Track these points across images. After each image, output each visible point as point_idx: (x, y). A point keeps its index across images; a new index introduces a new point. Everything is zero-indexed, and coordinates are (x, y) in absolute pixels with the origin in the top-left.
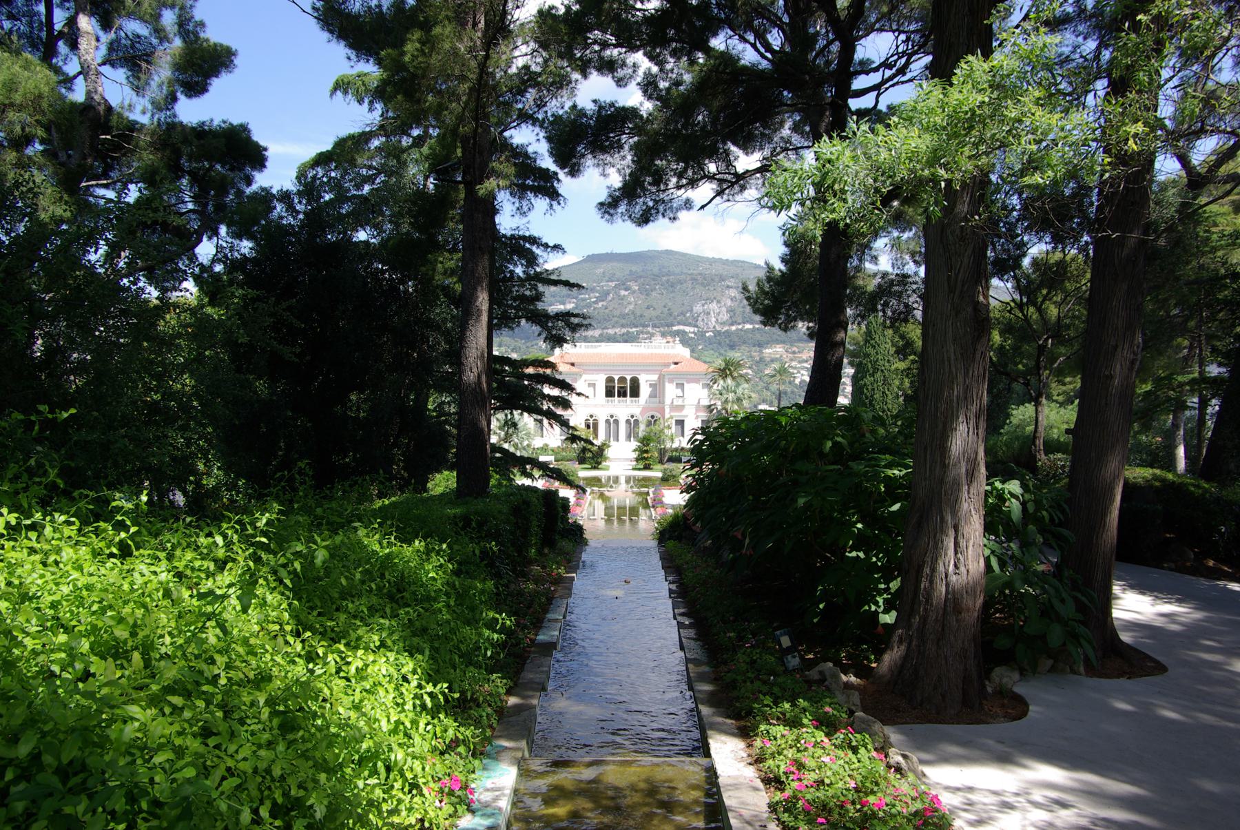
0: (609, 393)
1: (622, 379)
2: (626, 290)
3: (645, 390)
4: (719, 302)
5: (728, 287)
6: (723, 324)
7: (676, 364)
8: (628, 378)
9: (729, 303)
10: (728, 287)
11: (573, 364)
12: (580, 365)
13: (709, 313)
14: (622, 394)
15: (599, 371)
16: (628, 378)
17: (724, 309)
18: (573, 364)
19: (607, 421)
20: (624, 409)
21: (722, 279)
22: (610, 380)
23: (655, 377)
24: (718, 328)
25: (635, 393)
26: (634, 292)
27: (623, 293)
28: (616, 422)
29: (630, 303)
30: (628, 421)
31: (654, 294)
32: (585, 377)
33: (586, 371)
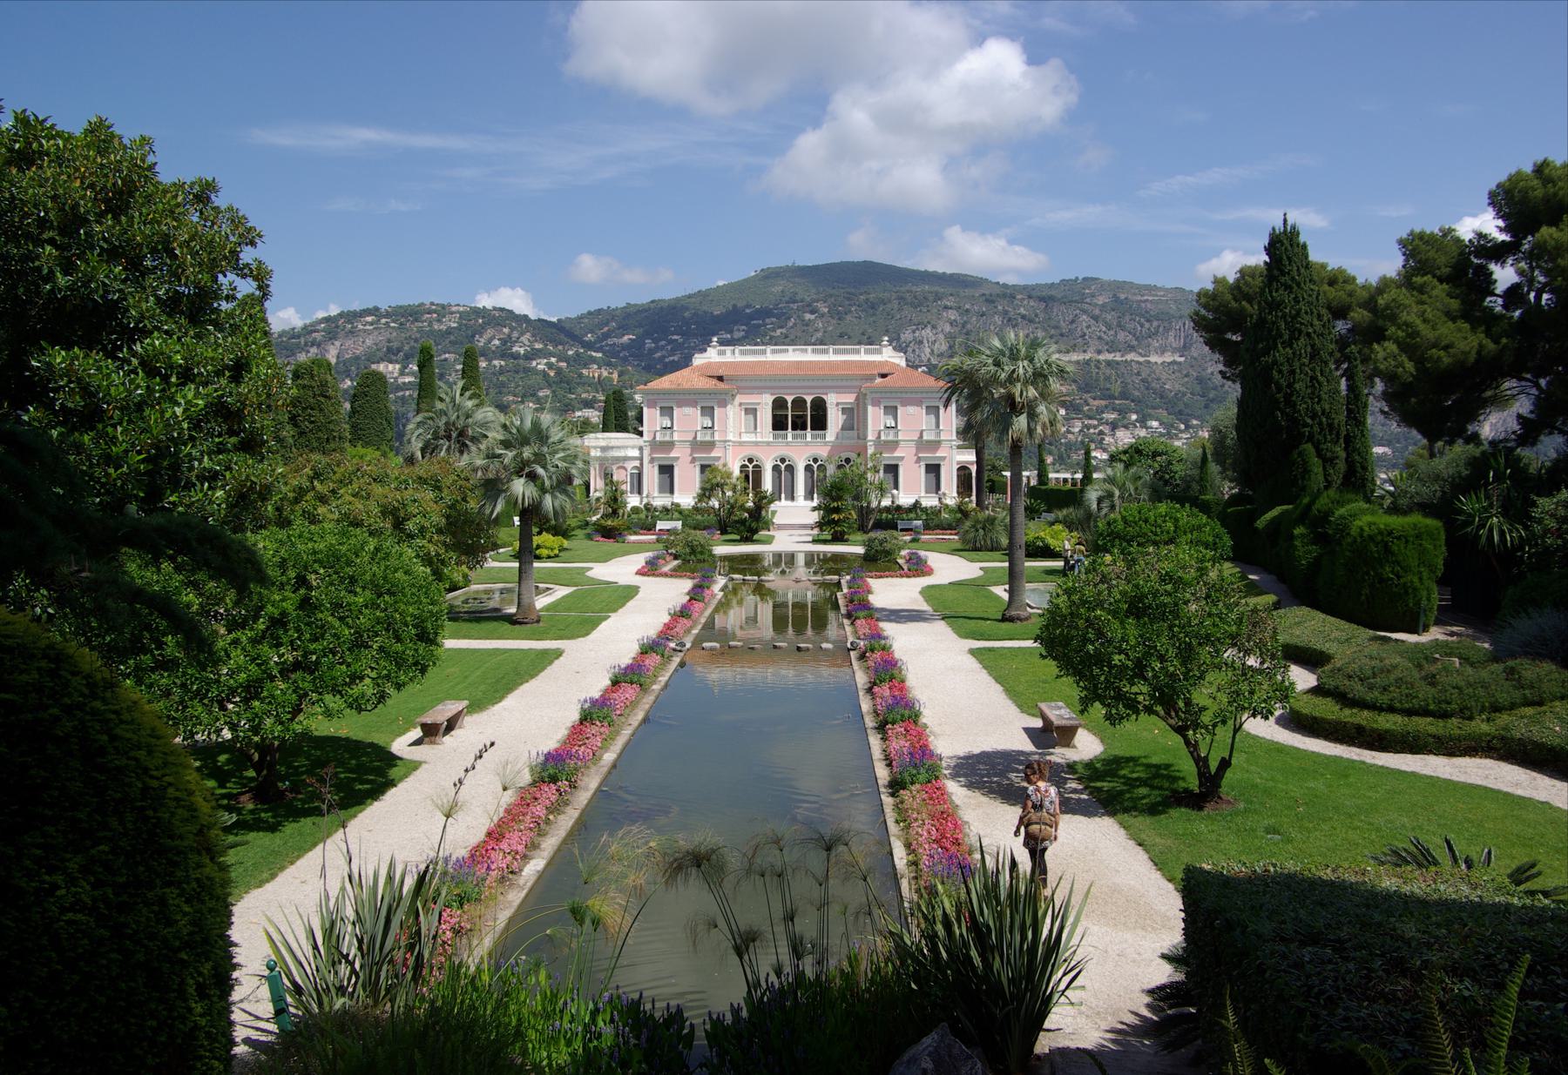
0: (779, 424)
1: (800, 403)
2: (812, 312)
3: (835, 419)
4: (934, 327)
5: (946, 307)
6: (941, 355)
7: (884, 376)
8: (809, 399)
9: (948, 328)
10: (946, 307)
11: (720, 379)
12: (732, 379)
13: (921, 342)
14: (799, 425)
15: (760, 390)
16: (809, 399)
17: (941, 336)
18: (720, 379)
19: (776, 468)
20: (803, 449)
21: (938, 297)
22: (779, 404)
23: (849, 398)
24: (934, 362)
25: (820, 423)
26: (823, 315)
27: (808, 316)
28: (791, 469)
29: (817, 330)
30: (808, 468)
31: (848, 317)
32: (739, 399)
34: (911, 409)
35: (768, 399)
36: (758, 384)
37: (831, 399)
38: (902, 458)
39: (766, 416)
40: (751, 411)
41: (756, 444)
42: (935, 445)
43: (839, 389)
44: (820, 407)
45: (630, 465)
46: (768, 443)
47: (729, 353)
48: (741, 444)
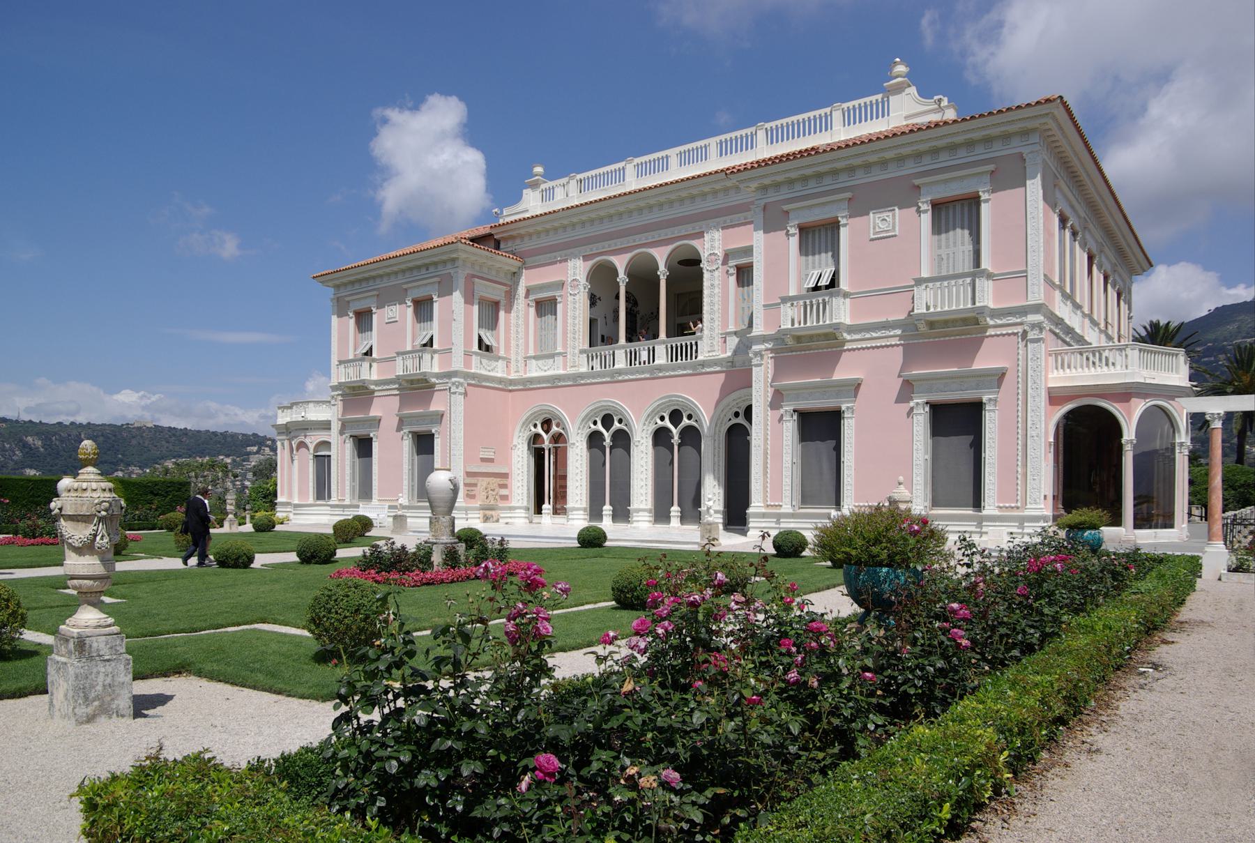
15: (559, 252)
16: (661, 256)
22: (602, 276)
28: (623, 440)
33: (525, 260)
34: (877, 221)
35: (577, 271)
36: (561, 238)
37: (712, 246)
38: (854, 388)
39: (575, 311)
40: (546, 307)
41: (554, 382)
42: (964, 331)
43: (727, 216)
44: (688, 270)
45: (312, 439)
46: (576, 380)
47: (559, 193)
48: (528, 385)
